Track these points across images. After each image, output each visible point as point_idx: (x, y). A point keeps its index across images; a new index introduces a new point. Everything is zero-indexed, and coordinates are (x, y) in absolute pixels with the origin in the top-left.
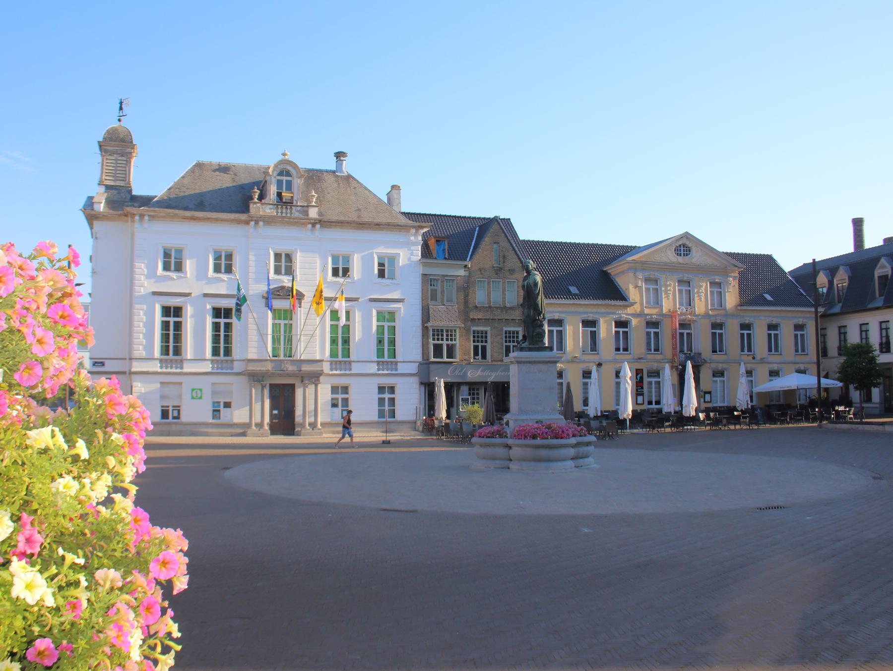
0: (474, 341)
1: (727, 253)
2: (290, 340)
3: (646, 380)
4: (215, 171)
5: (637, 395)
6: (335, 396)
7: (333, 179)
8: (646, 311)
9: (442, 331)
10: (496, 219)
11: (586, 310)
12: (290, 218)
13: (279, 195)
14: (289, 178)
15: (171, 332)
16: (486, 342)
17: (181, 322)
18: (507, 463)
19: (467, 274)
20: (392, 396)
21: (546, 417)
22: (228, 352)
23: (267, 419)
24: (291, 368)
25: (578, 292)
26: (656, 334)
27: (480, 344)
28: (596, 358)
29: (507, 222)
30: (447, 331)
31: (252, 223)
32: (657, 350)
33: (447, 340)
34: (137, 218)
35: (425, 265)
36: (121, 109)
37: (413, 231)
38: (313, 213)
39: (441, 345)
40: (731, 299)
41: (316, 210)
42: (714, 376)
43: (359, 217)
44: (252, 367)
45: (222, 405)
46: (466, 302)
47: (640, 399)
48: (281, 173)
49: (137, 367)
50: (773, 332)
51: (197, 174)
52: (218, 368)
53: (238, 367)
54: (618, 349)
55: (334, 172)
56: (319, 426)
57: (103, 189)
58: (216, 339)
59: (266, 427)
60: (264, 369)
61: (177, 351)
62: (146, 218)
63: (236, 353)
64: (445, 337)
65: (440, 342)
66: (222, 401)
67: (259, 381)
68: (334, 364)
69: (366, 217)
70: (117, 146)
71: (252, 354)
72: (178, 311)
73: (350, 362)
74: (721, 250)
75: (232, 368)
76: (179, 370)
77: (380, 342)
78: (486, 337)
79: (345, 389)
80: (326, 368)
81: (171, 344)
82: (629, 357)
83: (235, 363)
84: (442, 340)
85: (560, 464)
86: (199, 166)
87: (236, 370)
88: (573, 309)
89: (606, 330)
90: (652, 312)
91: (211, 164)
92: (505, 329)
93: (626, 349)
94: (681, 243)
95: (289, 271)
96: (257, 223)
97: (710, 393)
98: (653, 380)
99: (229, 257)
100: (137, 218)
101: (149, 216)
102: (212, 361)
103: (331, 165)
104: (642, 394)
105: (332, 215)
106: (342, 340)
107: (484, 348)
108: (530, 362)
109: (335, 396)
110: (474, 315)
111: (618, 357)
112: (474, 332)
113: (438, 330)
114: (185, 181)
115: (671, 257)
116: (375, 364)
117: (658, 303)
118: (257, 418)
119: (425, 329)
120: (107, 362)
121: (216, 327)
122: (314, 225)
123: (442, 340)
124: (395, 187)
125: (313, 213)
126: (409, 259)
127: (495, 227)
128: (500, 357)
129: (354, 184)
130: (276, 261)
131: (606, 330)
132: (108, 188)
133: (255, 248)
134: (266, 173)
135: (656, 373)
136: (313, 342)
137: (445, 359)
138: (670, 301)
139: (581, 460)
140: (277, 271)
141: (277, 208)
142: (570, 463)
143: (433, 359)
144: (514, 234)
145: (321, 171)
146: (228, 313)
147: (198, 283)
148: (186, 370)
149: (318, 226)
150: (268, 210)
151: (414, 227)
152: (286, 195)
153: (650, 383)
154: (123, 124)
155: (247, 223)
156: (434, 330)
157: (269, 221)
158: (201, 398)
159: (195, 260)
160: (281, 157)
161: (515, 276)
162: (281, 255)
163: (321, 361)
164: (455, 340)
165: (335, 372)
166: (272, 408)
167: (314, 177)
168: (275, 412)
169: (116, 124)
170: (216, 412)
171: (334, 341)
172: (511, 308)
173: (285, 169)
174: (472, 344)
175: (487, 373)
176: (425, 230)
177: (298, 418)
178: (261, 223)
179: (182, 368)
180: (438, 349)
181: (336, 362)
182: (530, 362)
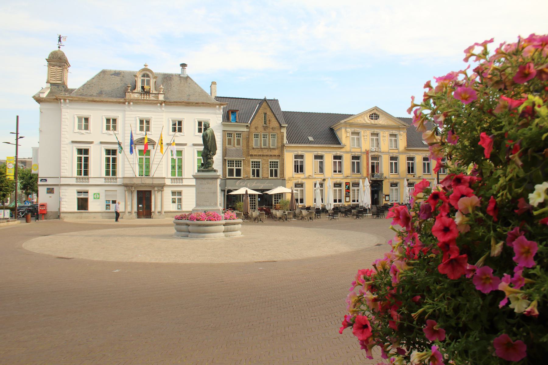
0: (252, 167)
1: (399, 118)
2: (148, 167)
3: (351, 188)
4: (112, 75)
5: (346, 196)
6: (174, 197)
7: (178, 79)
8: (353, 150)
9: (233, 161)
10: (265, 100)
11: (316, 150)
12: (147, 100)
13: (143, 88)
14: (148, 78)
15: (83, 163)
16: (259, 167)
17: (88, 158)
18: (187, 233)
19: (248, 130)
20: (180, 197)
21: (211, 208)
22: (114, 173)
23: (135, 209)
25: (313, 140)
26: (358, 163)
27: (256, 169)
28: (322, 176)
29: (276, 101)
30: (236, 161)
31: (127, 103)
32: (358, 171)
33: (236, 166)
34: (62, 101)
35: (224, 125)
36: (60, 41)
37: (218, 106)
38: (161, 97)
39: (233, 169)
40: (402, 142)
41: (163, 95)
42: (391, 186)
43: (188, 99)
44: (127, 182)
45: (111, 202)
46: (248, 146)
47: (348, 199)
48: (144, 76)
49: (63, 181)
50: (426, 162)
51: (101, 77)
53: (119, 182)
54: (335, 171)
55: (180, 75)
56: (163, 213)
57: (49, 85)
59: (135, 215)
61: (86, 173)
62: (67, 101)
63: (120, 174)
64: (235, 165)
65: (232, 168)
66: (111, 199)
69: (193, 99)
70: (58, 61)
71: (129, 174)
72: (86, 151)
73: (182, 179)
74: (396, 116)
78: (259, 165)
80: (168, 182)
81: (83, 169)
82: (341, 176)
84: (233, 166)
85: (211, 234)
86: (104, 72)
87: (118, 184)
88: (309, 150)
89: (328, 161)
90: (356, 151)
91: (110, 71)
92: (270, 160)
93: (340, 172)
94: (373, 112)
95: (148, 129)
96: (129, 103)
97: (388, 195)
98: (356, 188)
99: (115, 121)
100: (62, 101)
101: (69, 100)
103: (178, 70)
104: (349, 196)
105: (173, 98)
106: (177, 167)
107: (258, 171)
108: (202, 178)
109: (174, 197)
110: (252, 152)
111: (335, 176)
112: (252, 162)
113: (231, 161)
114: (94, 81)
115: (368, 120)
117: (359, 145)
118: (129, 209)
119: (224, 160)
120: (48, 179)
122: (161, 104)
123: (233, 166)
124: (214, 83)
125: (161, 97)
127: (264, 104)
128: (267, 176)
129: (189, 81)
131: (328, 161)
132: (52, 84)
133: (129, 118)
134: (135, 76)
135: (357, 184)
136: (161, 168)
137: (235, 177)
138: (366, 143)
139: (233, 232)
140: (141, 129)
141: (141, 95)
142: (222, 234)
143: (228, 177)
144: (279, 108)
145: (172, 75)
146: (114, 152)
147: (98, 137)
148: (90, 183)
149: (163, 104)
150: (136, 96)
151: (218, 105)
152: (146, 87)
153: (354, 190)
154: (61, 49)
155: (124, 103)
156: (228, 161)
157: (137, 102)
158: (99, 198)
160: (144, 67)
161: (275, 131)
163: (165, 178)
164: (241, 166)
166: (139, 203)
167: (167, 78)
168: (140, 206)
169: (57, 49)
170: (108, 206)
171: (173, 167)
172: (273, 149)
173: (146, 73)
174: (251, 169)
175: (258, 184)
176: (225, 106)
177: (153, 210)
178: (131, 103)
180: (231, 172)
182: (202, 178)
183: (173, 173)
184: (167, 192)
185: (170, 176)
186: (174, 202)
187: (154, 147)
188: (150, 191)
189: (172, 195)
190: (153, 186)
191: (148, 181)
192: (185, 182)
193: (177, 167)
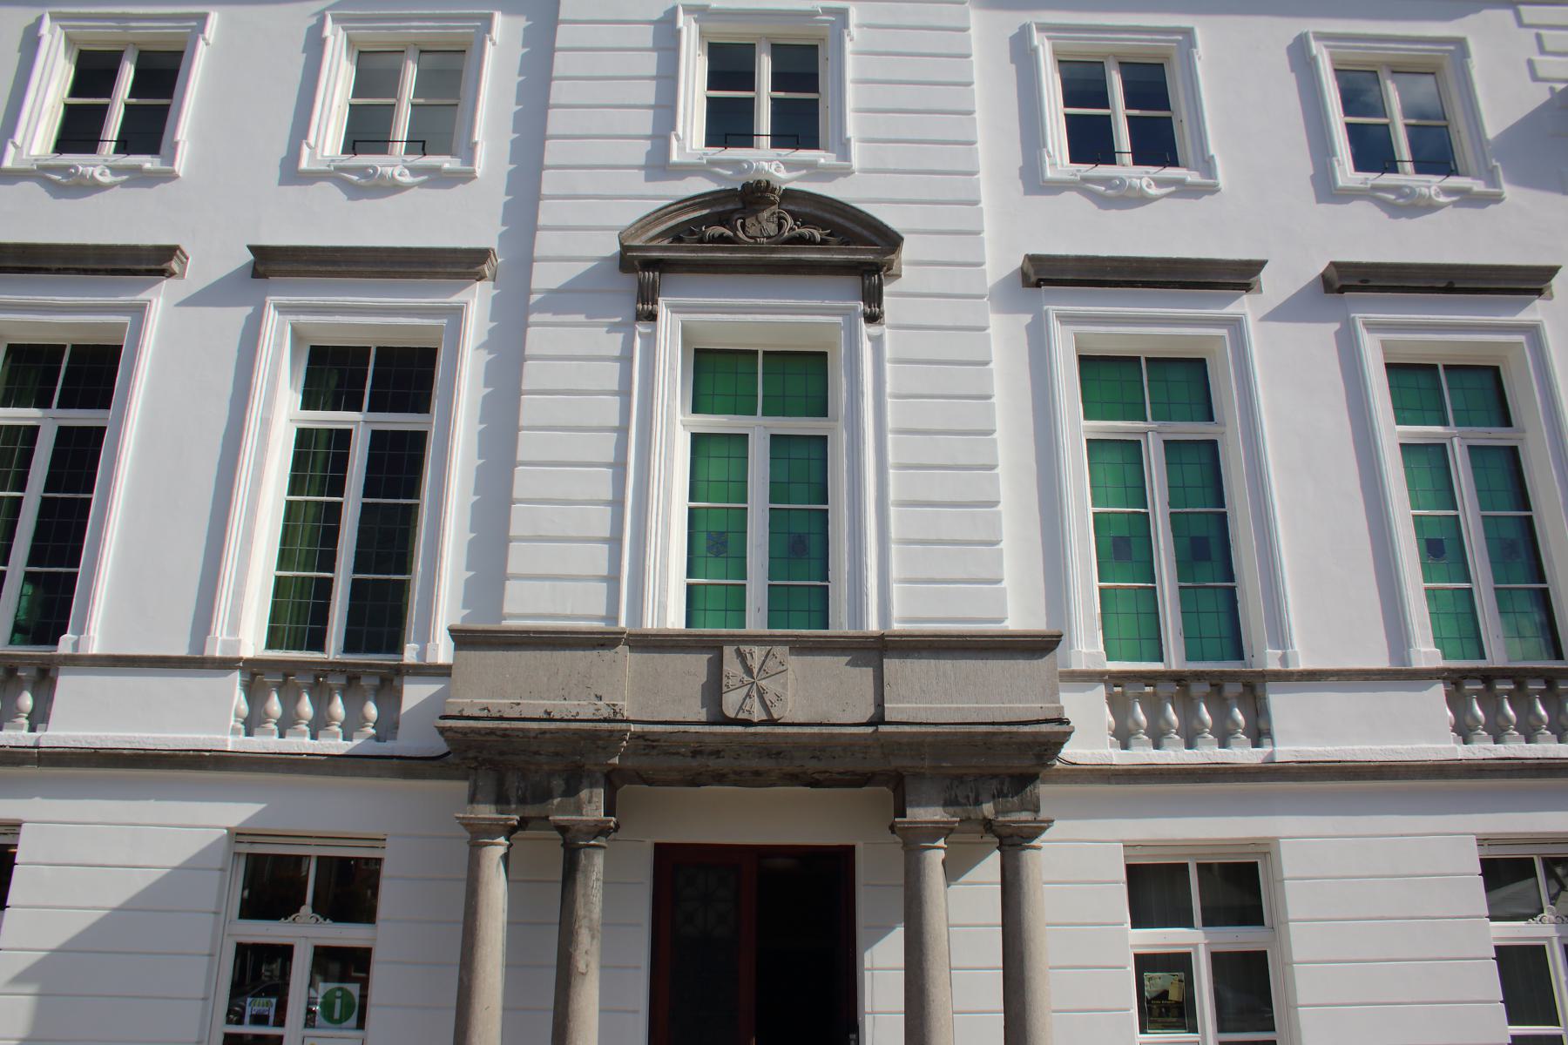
22: (382, 616)
58: (308, 535)
77: (1440, 548)
79: (1238, 888)
87: (401, 745)
95: (800, 126)
121: (317, 459)
136: (969, 507)
162: (745, 53)
183: (1132, 619)
184: (1080, 864)
185: (1086, 646)
186: (1163, 1010)
187: (873, 297)
188: (842, 859)
189: (1140, 919)
190: (889, 768)
191: (812, 695)
193: (1180, 523)
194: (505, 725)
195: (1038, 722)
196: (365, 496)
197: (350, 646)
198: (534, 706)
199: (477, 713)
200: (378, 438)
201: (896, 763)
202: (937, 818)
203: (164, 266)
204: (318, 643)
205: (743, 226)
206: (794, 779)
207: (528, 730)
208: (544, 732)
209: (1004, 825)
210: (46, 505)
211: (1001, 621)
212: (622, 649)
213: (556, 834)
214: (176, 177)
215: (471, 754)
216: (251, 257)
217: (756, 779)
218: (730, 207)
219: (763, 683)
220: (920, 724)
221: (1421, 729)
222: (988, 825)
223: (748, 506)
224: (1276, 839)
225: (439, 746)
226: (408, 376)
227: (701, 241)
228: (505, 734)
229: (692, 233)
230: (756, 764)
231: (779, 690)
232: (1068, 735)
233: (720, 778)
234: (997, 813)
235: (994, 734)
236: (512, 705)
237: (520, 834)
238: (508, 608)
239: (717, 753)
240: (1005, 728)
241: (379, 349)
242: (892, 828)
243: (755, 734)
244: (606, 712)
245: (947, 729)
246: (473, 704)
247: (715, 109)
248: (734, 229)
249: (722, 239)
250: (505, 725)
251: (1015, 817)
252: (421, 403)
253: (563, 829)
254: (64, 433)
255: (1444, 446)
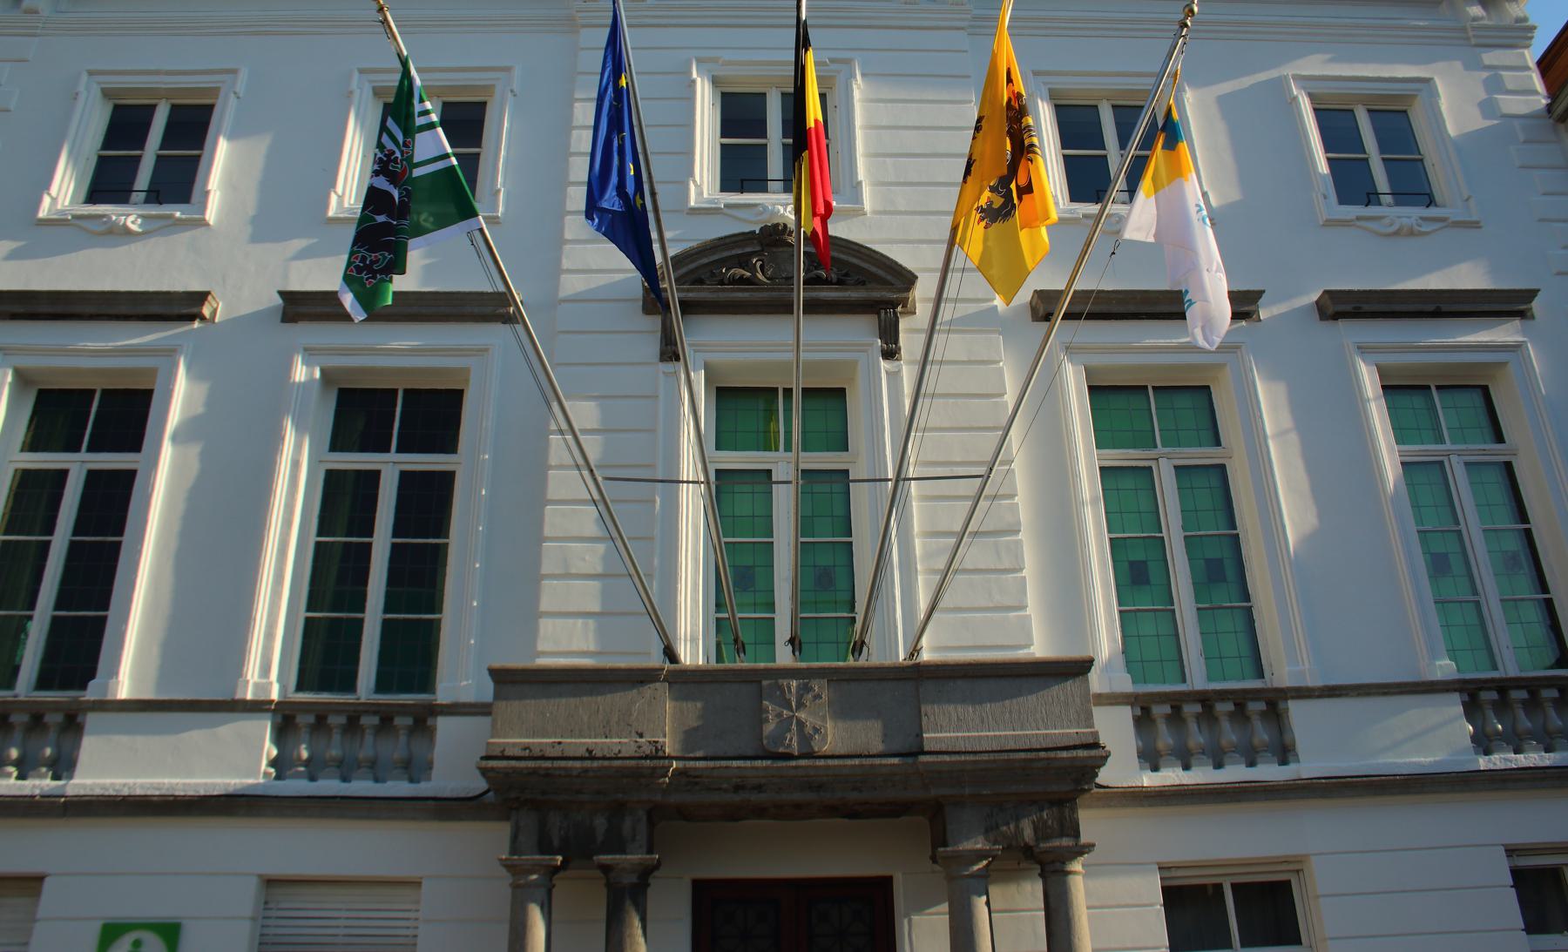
22: (412, 654)
24: (838, 736)
52: (314, 769)
58: (333, 576)
60: (620, 743)
63: (460, 674)
67: (578, 850)
68: (1165, 717)
72: (125, 415)
75: (414, 768)
76: (41, 784)
83: (443, 724)
102: (286, 720)
116: (1453, 707)
121: (344, 501)
126: (1488, 108)
130: (729, 125)
148: (87, 780)
159: (259, 147)
165: (1171, 776)
179: (63, 766)
181: (1176, 702)
192: (1324, 742)
194: (548, 764)
195: (1075, 747)
196: (394, 536)
197: (382, 685)
198: (577, 743)
199: (517, 752)
200: (407, 478)
201: (934, 792)
202: (979, 846)
203: (195, 310)
204: (349, 684)
205: (762, 267)
206: (832, 810)
207: (571, 769)
208: (586, 770)
209: (1046, 852)
210: (74, 548)
211: (1028, 646)
212: (662, 688)
213: (598, 873)
214: (207, 225)
215: (513, 795)
216: (280, 301)
217: (798, 811)
218: (749, 249)
219: (802, 715)
220: (958, 753)
221: (1438, 737)
222: (1028, 853)
223: (775, 540)
224: (1307, 856)
225: (479, 785)
226: (434, 415)
227: (722, 283)
228: (548, 774)
229: (713, 274)
230: (797, 796)
231: (818, 723)
232: (1106, 758)
233: (760, 812)
234: (1037, 840)
235: (1031, 760)
236: (553, 745)
237: (561, 874)
238: (541, 647)
239: (759, 788)
240: (1042, 754)
241: (406, 391)
242: (934, 859)
243: (796, 767)
244: (647, 750)
245: (985, 757)
246: (514, 744)
247: (729, 156)
248: (752, 269)
249: (742, 280)
250: (548, 764)
251: (1056, 843)
252: (446, 441)
253: (606, 869)
254: (93, 477)
255: (1441, 463)
